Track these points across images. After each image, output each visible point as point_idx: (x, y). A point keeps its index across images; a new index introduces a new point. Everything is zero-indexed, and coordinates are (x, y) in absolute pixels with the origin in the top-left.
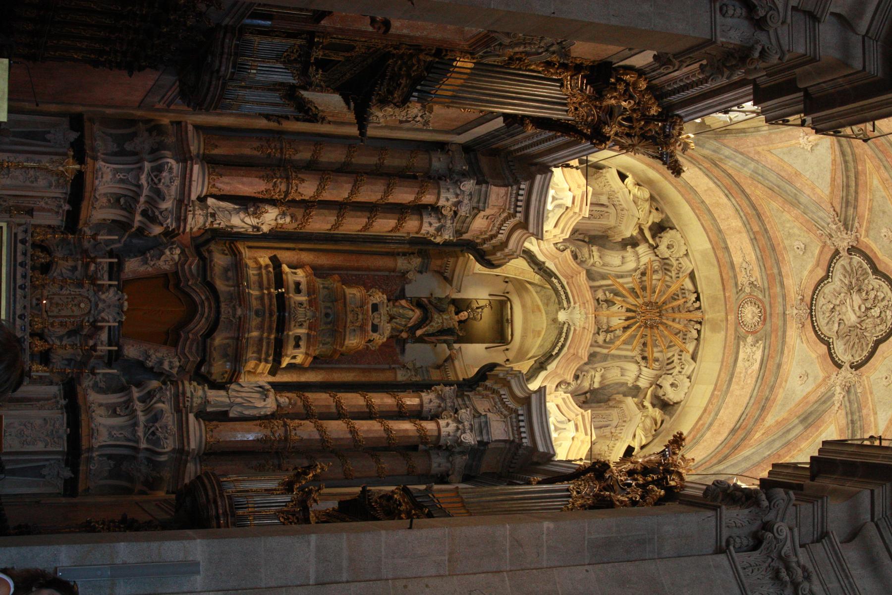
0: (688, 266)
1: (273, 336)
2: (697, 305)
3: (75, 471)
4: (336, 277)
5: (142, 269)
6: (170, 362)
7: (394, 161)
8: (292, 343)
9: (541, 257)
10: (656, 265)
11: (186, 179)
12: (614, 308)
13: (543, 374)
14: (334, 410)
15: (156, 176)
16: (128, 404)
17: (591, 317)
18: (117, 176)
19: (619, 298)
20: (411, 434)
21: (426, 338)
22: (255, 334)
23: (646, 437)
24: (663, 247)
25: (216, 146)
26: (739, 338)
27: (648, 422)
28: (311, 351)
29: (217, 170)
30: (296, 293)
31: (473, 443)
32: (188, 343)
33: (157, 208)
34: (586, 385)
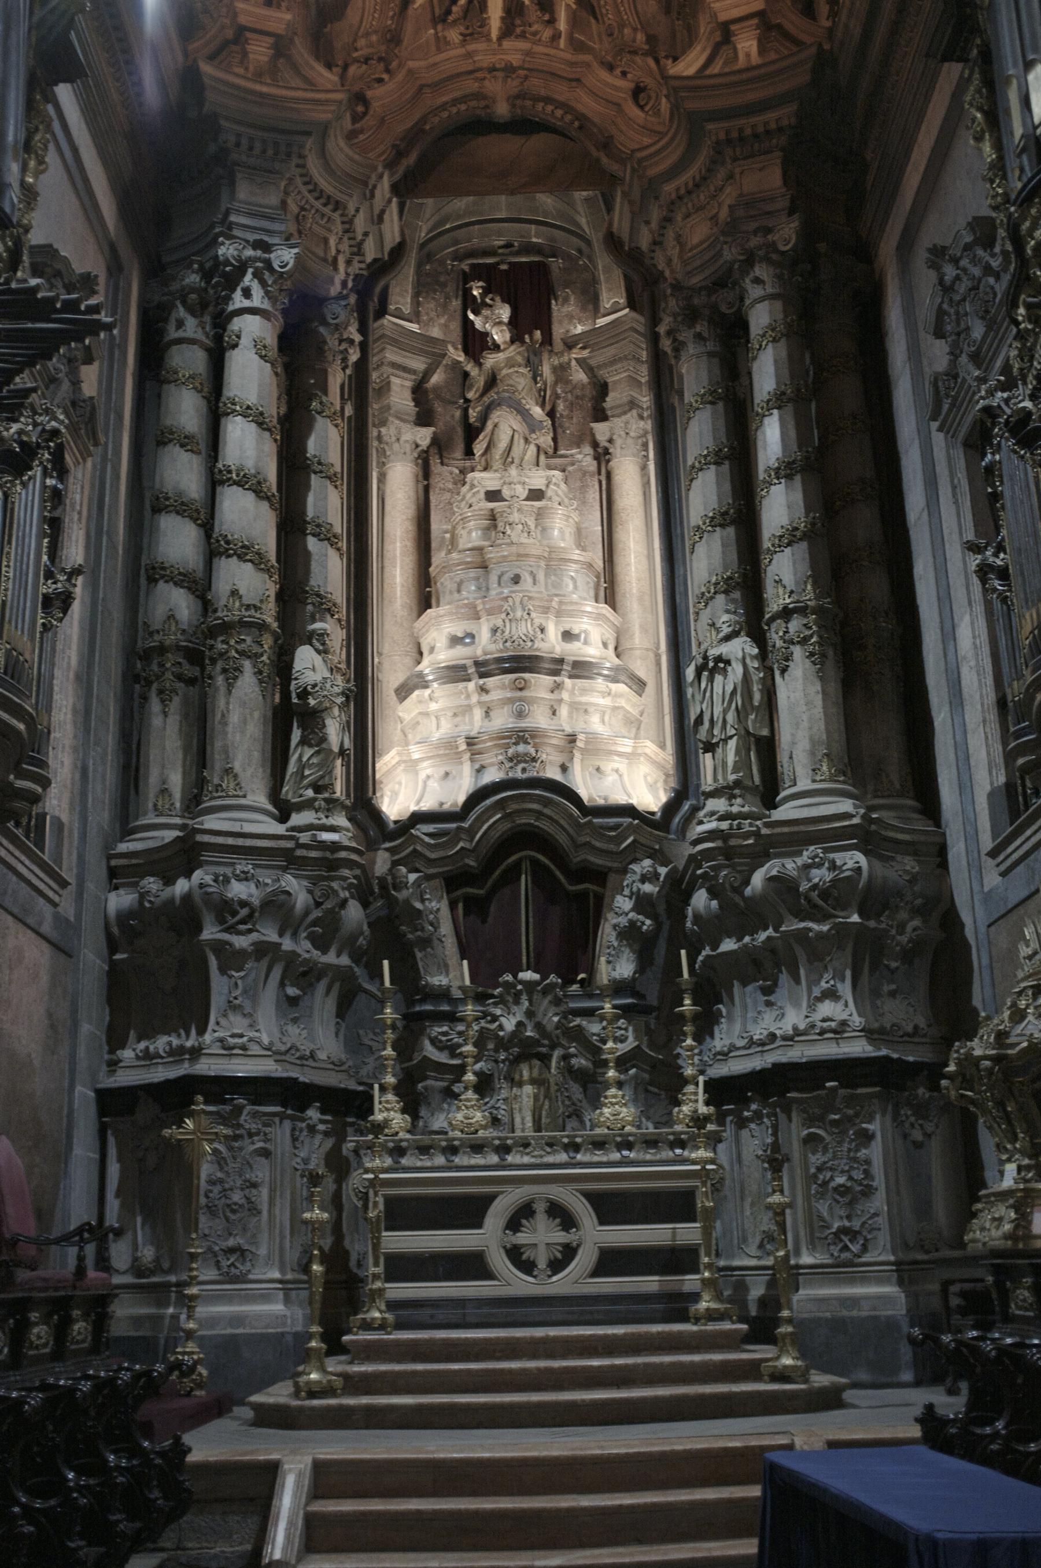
6: (644, 879)
15: (234, 914)
18: (237, 1002)
20: (784, 354)
21: (548, 408)
29: (216, 781)
30: (473, 643)
31: (797, 223)
32: (598, 844)
33: (307, 913)
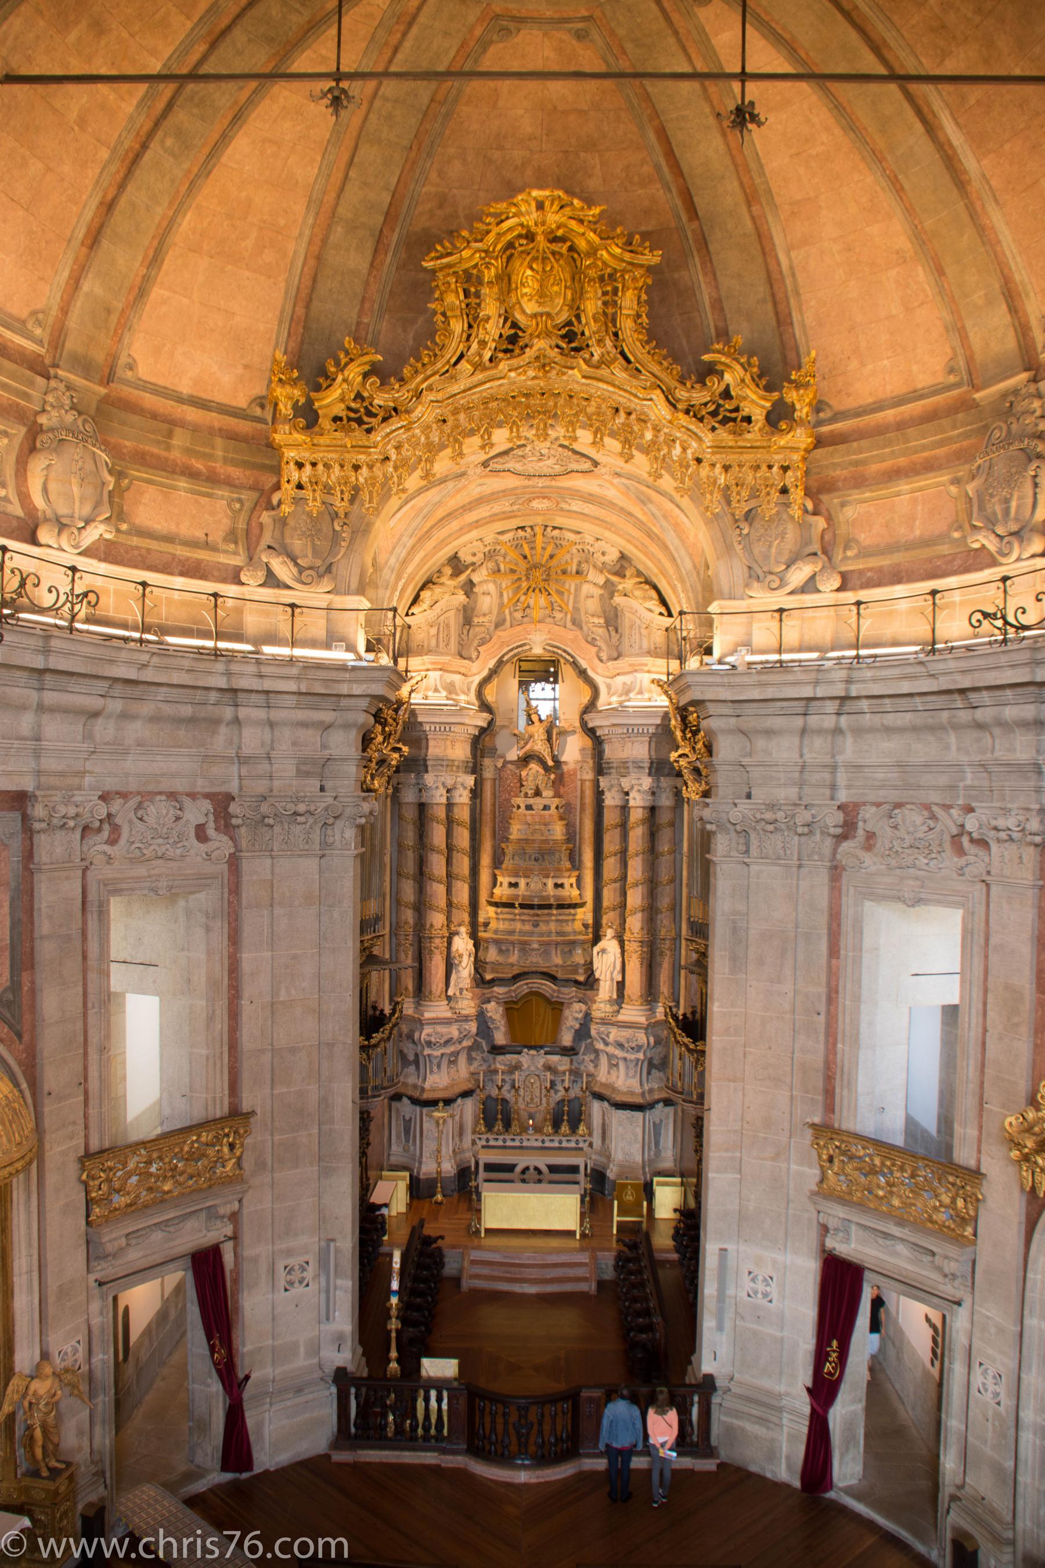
0: (489, 539)
1: (555, 912)
2: (529, 530)
3: (657, 1102)
4: (503, 845)
5: (503, 1029)
7: (410, 837)
8: (560, 892)
9: (485, 673)
10: (491, 565)
11: (436, 1022)
12: (532, 602)
13: (590, 673)
14: (618, 885)
16: (610, 1057)
17: (539, 626)
19: (523, 598)
22: (553, 927)
23: (652, 599)
24: (474, 559)
25: (406, 989)
26: (562, 510)
27: (637, 593)
28: (567, 874)
34: (601, 631)
